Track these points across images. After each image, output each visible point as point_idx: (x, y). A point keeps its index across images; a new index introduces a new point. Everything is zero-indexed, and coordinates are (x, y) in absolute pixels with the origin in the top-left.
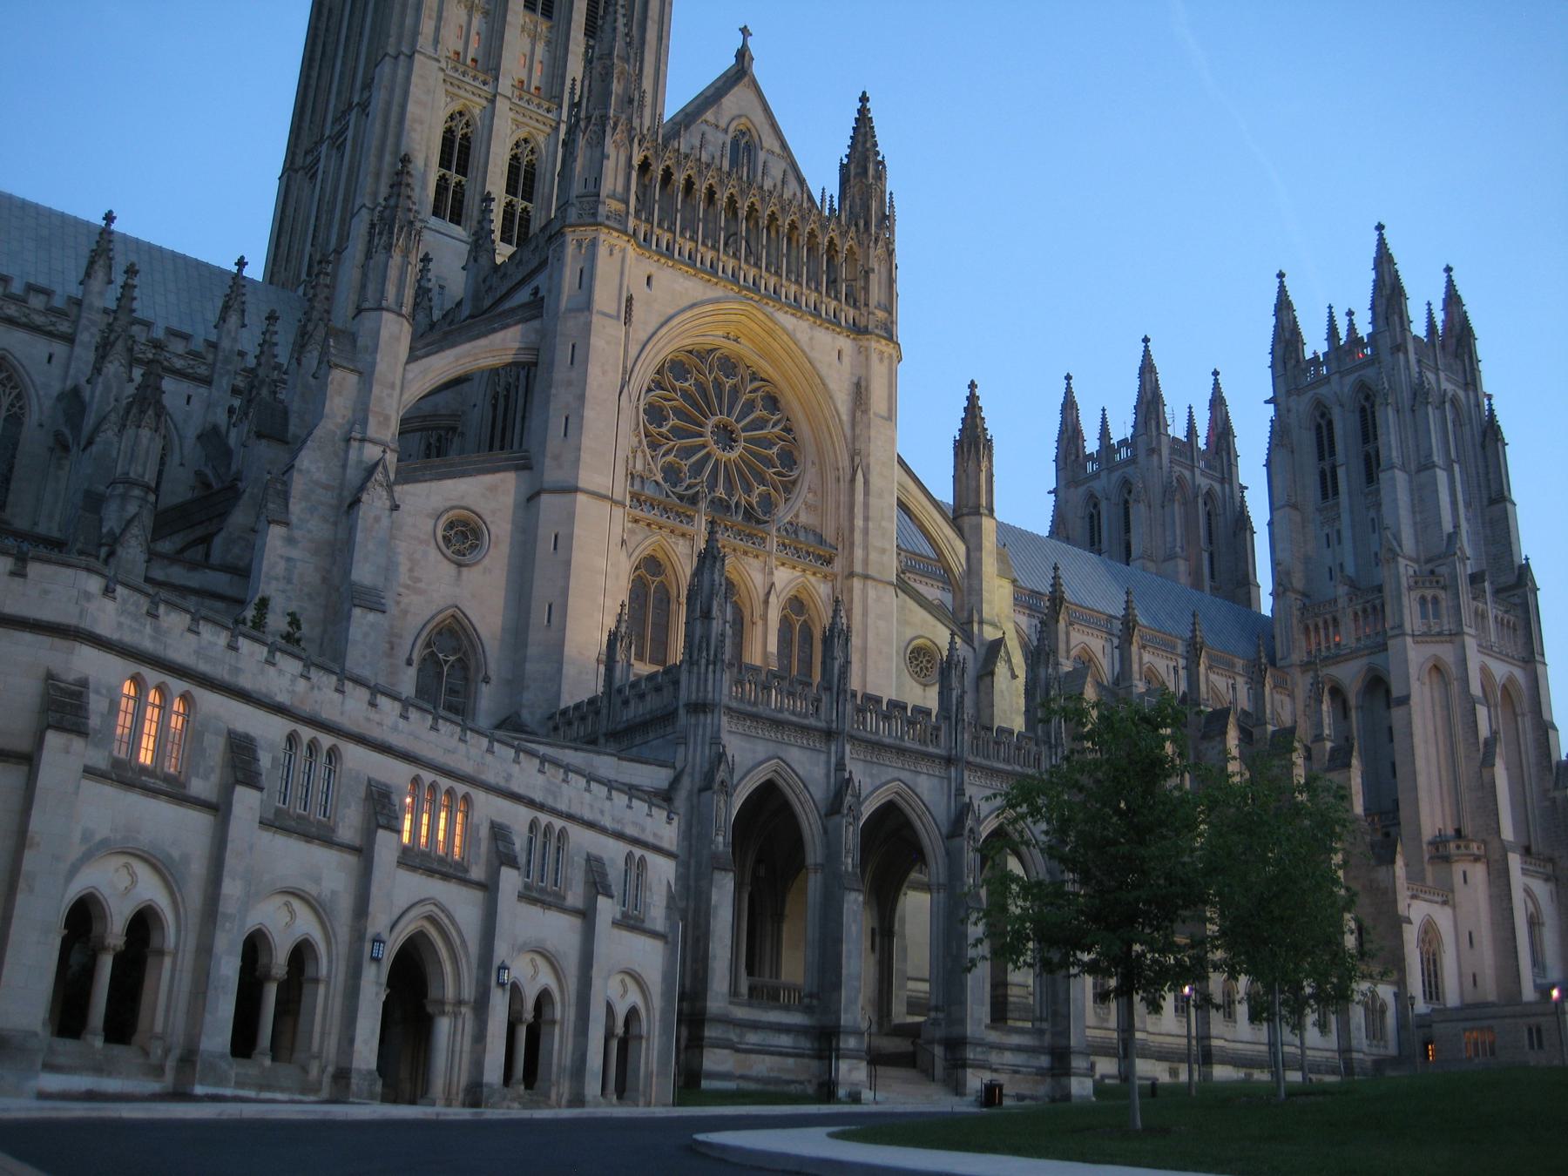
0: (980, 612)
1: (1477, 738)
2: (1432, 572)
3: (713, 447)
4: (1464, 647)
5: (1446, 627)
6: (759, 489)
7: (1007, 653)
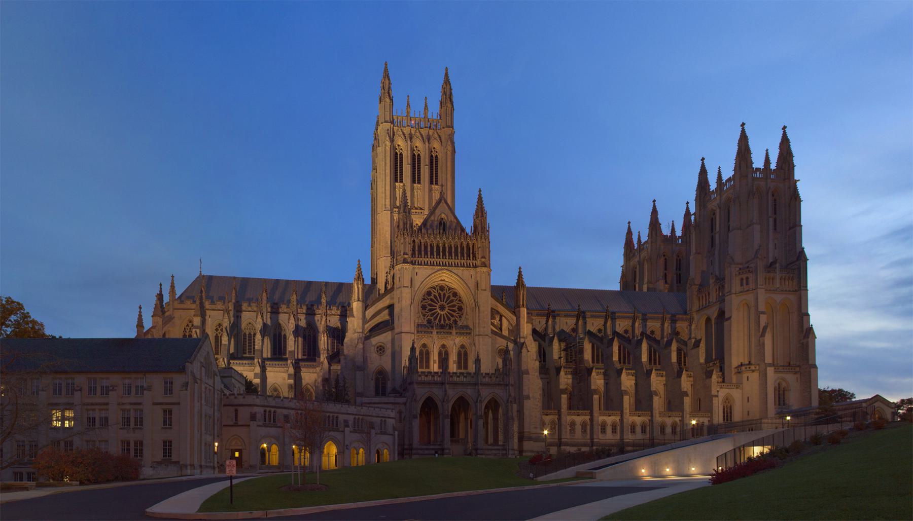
0: (520, 335)
1: (759, 326)
2: (748, 267)
3: (439, 312)
4: (757, 294)
5: (751, 287)
6: (452, 319)
7: (526, 345)
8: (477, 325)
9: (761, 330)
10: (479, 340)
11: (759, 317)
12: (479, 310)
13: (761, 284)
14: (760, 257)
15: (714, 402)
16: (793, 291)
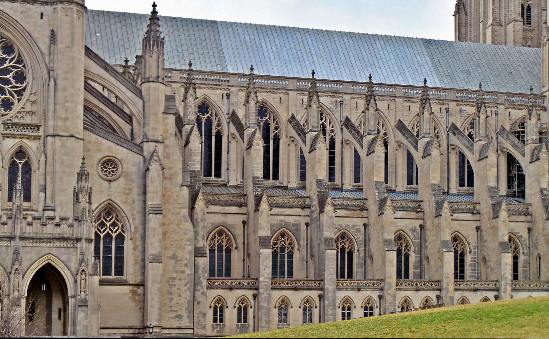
8: (51, 114)
10: (54, 143)
12: (55, 84)
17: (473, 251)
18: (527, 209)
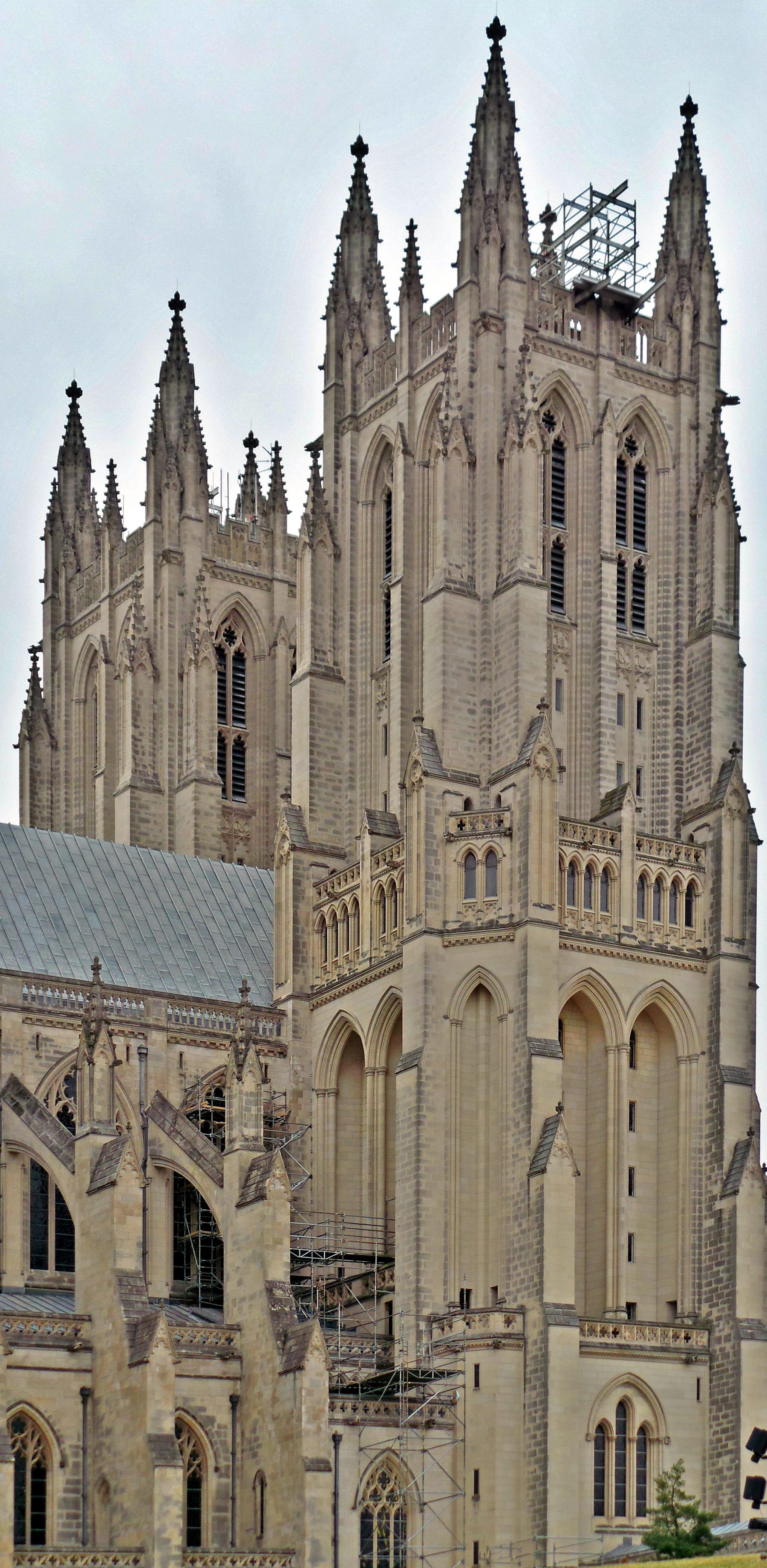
9: (536, 1133)
11: (530, 1067)
13: (546, 901)
14: (542, 761)
15: (309, 1494)
16: (693, 954)
17: (71, 1460)
18: (230, 1340)
